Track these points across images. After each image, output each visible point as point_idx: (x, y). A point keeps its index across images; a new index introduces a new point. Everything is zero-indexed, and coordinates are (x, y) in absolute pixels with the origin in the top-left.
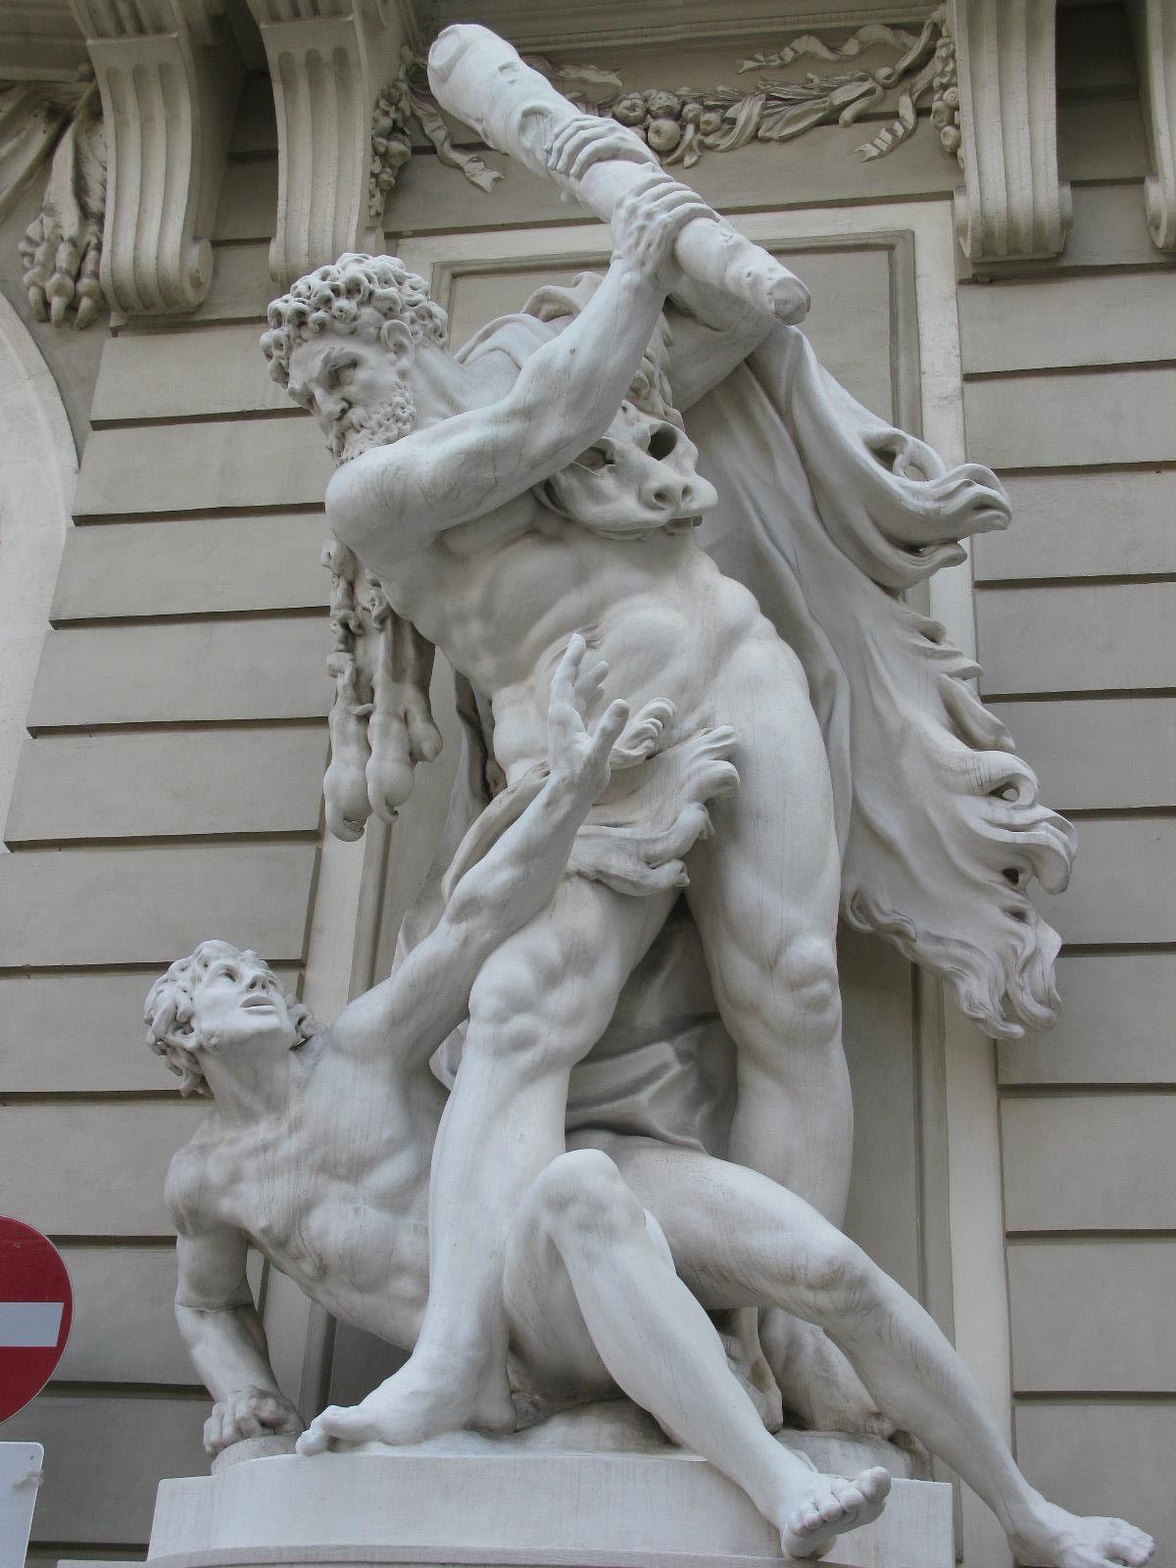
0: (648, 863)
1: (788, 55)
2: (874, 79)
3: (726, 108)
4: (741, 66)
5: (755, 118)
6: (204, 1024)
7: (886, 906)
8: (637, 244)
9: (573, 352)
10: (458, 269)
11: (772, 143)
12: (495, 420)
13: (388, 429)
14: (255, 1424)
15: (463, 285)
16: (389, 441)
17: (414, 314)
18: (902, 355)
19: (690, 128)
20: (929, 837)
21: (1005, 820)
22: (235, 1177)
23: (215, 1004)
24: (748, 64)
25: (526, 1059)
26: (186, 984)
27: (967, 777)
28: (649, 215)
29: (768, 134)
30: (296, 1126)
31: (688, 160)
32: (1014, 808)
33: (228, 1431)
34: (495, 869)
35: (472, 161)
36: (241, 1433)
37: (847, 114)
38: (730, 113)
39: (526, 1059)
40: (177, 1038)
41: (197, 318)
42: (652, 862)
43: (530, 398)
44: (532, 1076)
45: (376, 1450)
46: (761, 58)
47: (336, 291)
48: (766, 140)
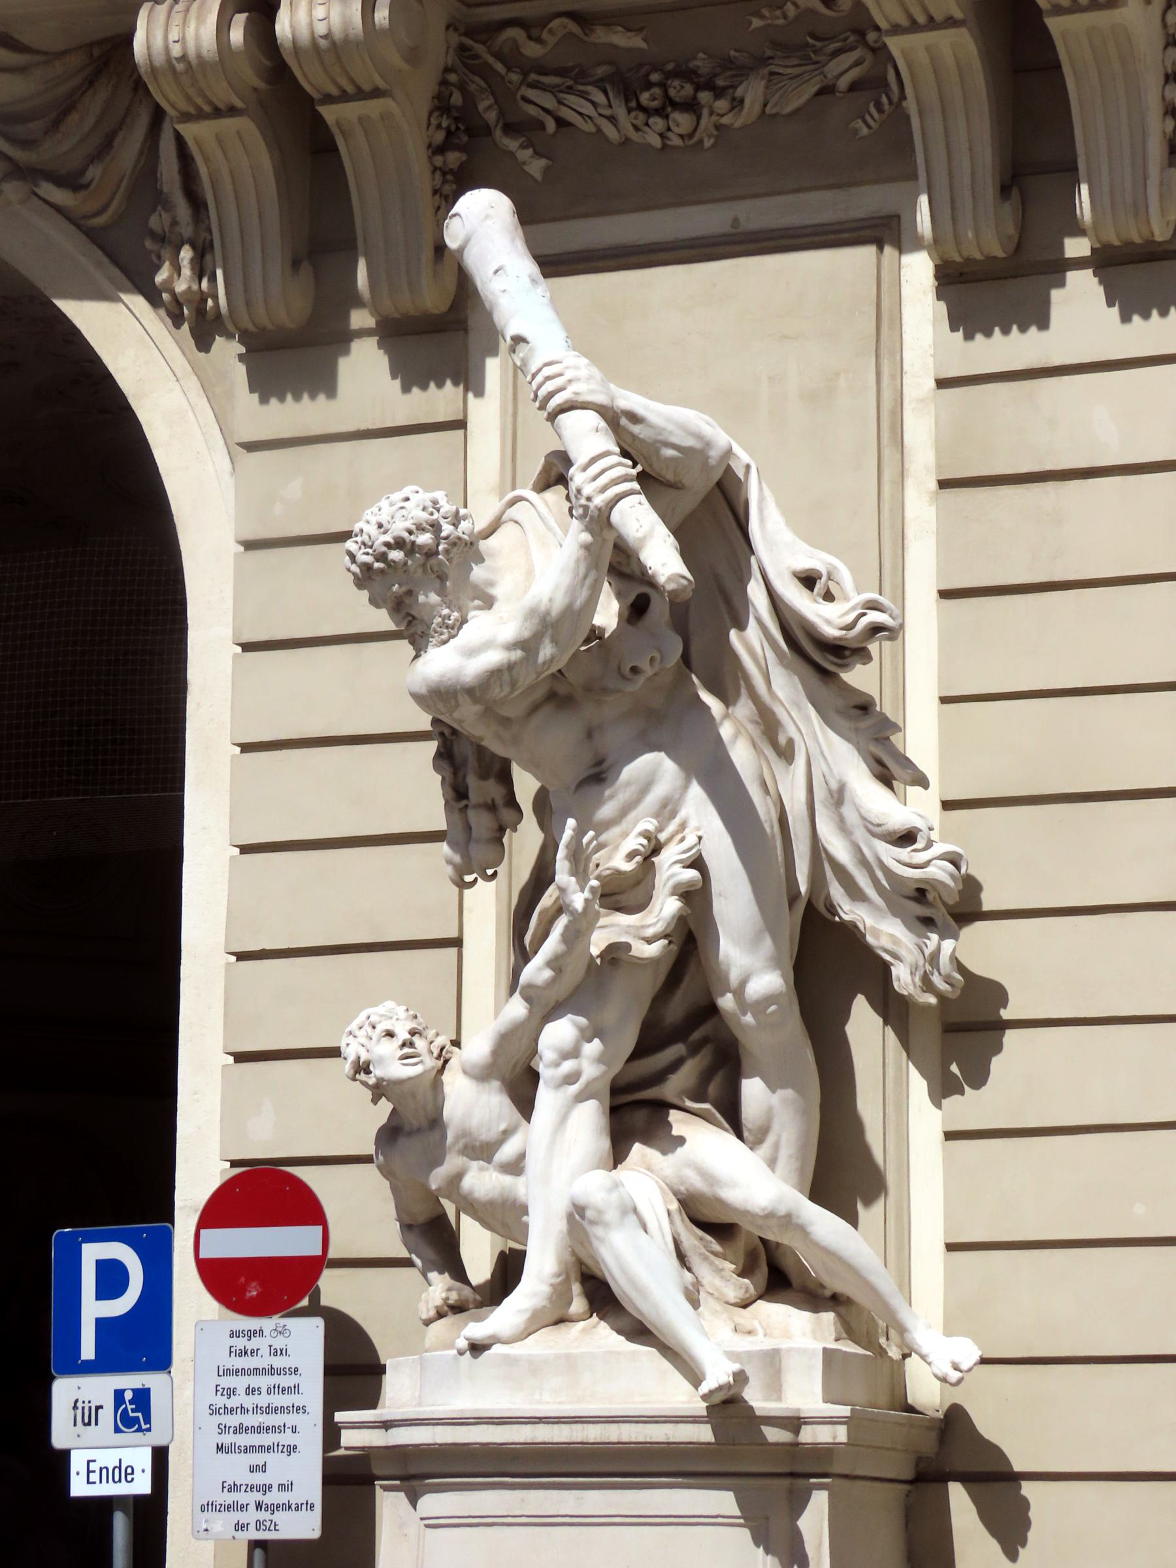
0: (647, 941)
2: (866, 44)
3: (734, 87)
4: (750, 23)
5: (761, 100)
6: (377, 1072)
7: (846, 907)
9: (551, 600)
13: (442, 634)
14: (446, 1308)
16: (445, 642)
17: (446, 546)
18: (886, 361)
19: (705, 112)
20: (864, 862)
21: (907, 860)
24: (756, 23)
25: (574, 1089)
26: (363, 1040)
27: (880, 828)
28: (589, 499)
29: (774, 111)
31: (708, 143)
32: (914, 851)
33: (432, 1313)
34: (540, 969)
35: (522, 147)
36: (440, 1315)
38: (739, 92)
39: (574, 1089)
40: (362, 1076)
42: (649, 941)
43: (526, 634)
44: (580, 1098)
45: (497, 1349)
47: (387, 545)
48: (775, 116)
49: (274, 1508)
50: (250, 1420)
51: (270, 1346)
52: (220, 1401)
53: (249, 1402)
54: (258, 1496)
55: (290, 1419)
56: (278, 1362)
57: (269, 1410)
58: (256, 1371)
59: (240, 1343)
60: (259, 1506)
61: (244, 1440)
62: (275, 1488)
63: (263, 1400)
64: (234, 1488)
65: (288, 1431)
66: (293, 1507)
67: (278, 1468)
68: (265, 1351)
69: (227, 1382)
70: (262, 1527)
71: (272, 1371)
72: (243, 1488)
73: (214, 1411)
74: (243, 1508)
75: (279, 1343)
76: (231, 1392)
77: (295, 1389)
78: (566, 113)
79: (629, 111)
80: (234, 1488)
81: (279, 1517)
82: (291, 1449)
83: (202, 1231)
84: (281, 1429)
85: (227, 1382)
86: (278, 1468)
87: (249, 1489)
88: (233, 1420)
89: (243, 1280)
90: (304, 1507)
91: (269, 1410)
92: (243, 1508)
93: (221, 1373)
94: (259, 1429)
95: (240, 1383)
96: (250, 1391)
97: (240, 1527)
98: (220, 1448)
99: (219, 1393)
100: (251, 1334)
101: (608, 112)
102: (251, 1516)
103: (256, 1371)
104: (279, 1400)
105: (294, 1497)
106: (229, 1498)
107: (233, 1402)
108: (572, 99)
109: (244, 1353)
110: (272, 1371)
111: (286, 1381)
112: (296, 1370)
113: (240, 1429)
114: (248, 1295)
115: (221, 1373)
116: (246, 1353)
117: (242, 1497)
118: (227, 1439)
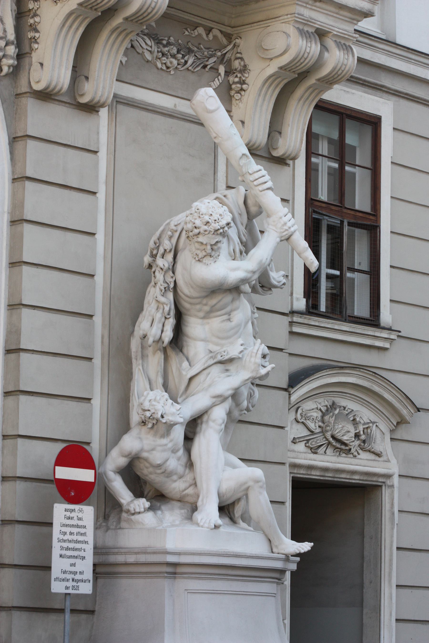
4: (184, 33)
8: (283, 232)
10: (118, 100)
11: (190, 72)
12: (247, 271)
15: (120, 107)
22: (153, 449)
23: (173, 414)
24: (187, 33)
28: (290, 228)
30: (171, 441)
31: (172, 72)
33: (142, 510)
34: (228, 390)
37: (209, 67)
41: (53, 97)
46: (189, 31)
49: (78, 581)
50: (71, 545)
51: (77, 516)
54: (72, 576)
55: (83, 546)
56: (80, 523)
57: (77, 542)
58: (73, 526)
59: (68, 514)
60: (73, 580)
61: (69, 553)
62: (78, 573)
63: (75, 538)
64: (65, 572)
65: (83, 551)
66: (84, 581)
68: (75, 518)
69: (64, 529)
70: (74, 588)
71: (78, 526)
72: (68, 572)
73: (59, 541)
74: (68, 580)
75: (80, 515)
76: (65, 533)
77: (84, 534)
78: (136, 44)
79: (158, 52)
81: (79, 584)
82: (83, 558)
83: (57, 467)
84: (79, 550)
85: (64, 529)
87: (70, 573)
88: (65, 545)
89: (69, 488)
90: (87, 581)
91: (77, 542)
92: (68, 580)
93: (62, 526)
95: (68, 530)
96: (71, 534)
97: (67, 588)
98: (61, 556)
99: (61, 534)
100: (73, 511)
101: (150, 49)
102: (70, 584)
103: (73, 526)
104: (80, 538)
105: (84, 577)
106: (63, 576)
107: (66, 538)
109: (69, 518)
110: (78, 526)
111: (82, 531)
112: (85, 526)
113: (68, 549)
114: (71, 495)
115: (62, 526)
116: (70, 518)
118: (64, 552)
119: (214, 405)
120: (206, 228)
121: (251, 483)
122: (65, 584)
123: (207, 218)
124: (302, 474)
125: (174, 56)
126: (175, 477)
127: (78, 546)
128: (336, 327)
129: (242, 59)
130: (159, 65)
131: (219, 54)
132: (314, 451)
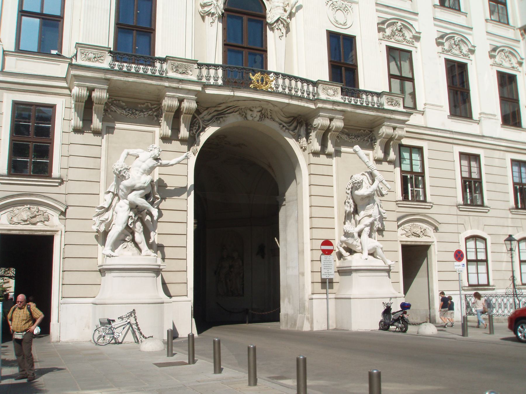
1: (361, 131)
49: (330, 275)
52: (324, 264)
53: (327, 264)
55: (331, 266)
56: (329, 260)
57: (329, 265)
59: (326, 258)
61: (326, 268)
64: (326, 273)
67: (330, 271)
69: (325, 262)
71: (329, 261)
75: (329, 258)
77: (331, 263)
78: (342, 137)
80: (326, 273)
82: (331, 269)
85: (325, 262)
86: (330, 271)
88: (325, 266)
91: (329, 265)
94: (328, 267)
95: (326, 262)
96: (327, 263)
97: (327, 277)
100: (327, 257)
107: (325, 264)
108: (343, 136)
110: (329, 261)
111: (330, 262)
113: (326, 267)
117: (327, 274)
118: (325, 268)
119: (365, 227)
120: (356, 181)
121: (376, 247)
122: (326, 276)
123: (356, 179)
124: (404, 243)
125: (354, 139)
126: (357, 247)
127: (329, 266)
128: (412, 204)
129: (374, 137)
130: (350, 141)
131: (368, 136)
132: (408, 236)
